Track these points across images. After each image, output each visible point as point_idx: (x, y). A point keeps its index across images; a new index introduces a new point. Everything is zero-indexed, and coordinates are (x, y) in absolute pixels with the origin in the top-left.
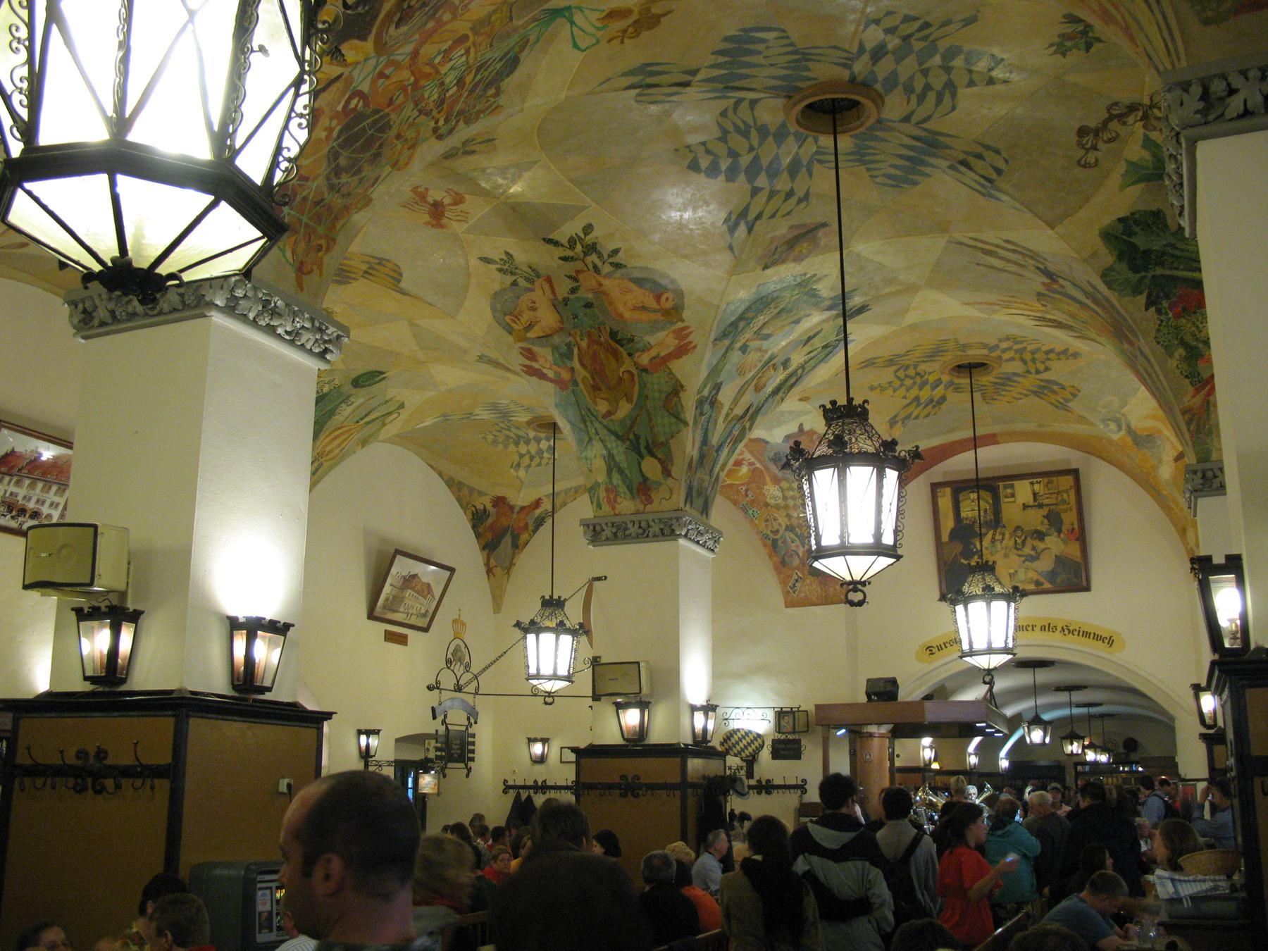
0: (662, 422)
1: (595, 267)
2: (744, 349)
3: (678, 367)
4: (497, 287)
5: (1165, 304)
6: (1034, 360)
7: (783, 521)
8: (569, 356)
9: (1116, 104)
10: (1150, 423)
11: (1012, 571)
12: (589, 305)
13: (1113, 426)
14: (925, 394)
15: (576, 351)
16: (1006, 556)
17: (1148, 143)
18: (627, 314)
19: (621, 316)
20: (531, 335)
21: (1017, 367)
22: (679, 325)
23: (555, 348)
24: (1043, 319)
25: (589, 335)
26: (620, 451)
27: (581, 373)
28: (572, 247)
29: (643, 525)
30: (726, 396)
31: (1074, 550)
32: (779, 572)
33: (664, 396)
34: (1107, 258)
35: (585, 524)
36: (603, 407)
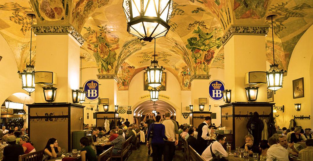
0: (112, 60)
1: (105, 32)
2: (126, 49)
3: (116, 51)
4: (86, 33)
5: (194, 51)
6: (165, 56)
8: (97, 47)
9: (196, 21)
10: (178, 67)
12: (103, 38)
13: (173, 67)
14: (147, 59)
15: (99, 46)
17: (198, 28)
18: (109, 41)
19: (108, 41)
20: (90, 42)
21: (162, 56)
22: (118, 44)
23: (95, 45)
24: (171, 50)
25: (102, 43)
26: (104, 64)
27: (99, 50)
28: (102, 28)
29: (108, 76)
30: (122, 56)
31: (164, 85)
32: (117, 85)
33: (113, 55)
34: (188, 43)
35: (97, 75)
36: (102, 56)
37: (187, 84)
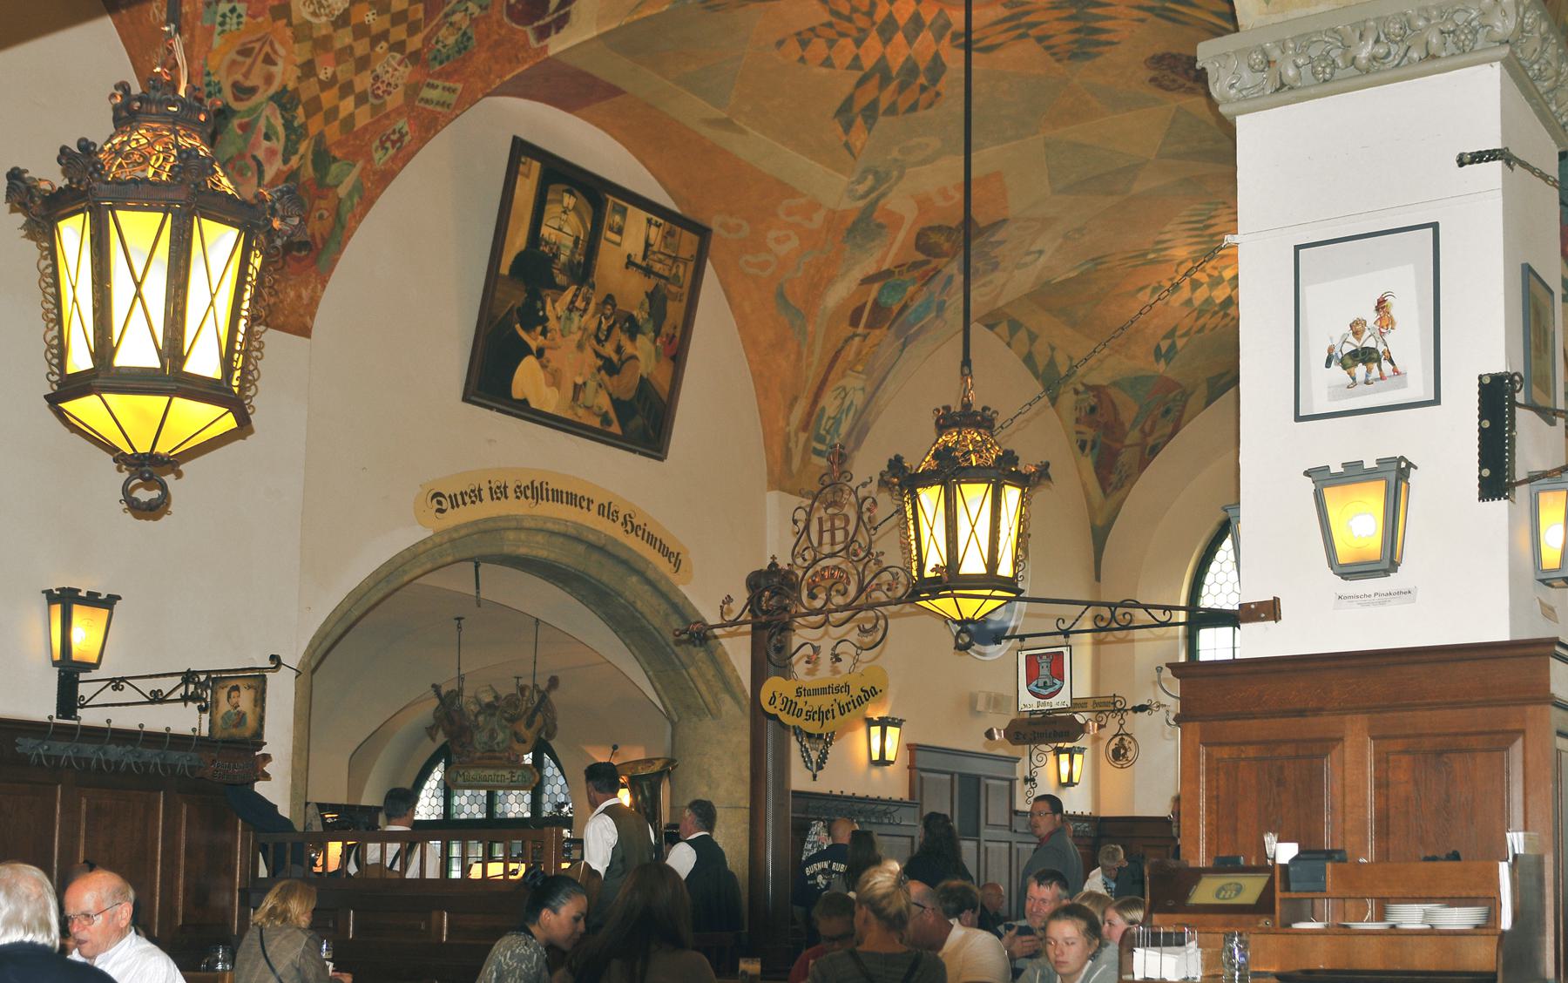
7: (285, 73)
11: (579, 381)
16: (580, 346)
37: (837, 421)
